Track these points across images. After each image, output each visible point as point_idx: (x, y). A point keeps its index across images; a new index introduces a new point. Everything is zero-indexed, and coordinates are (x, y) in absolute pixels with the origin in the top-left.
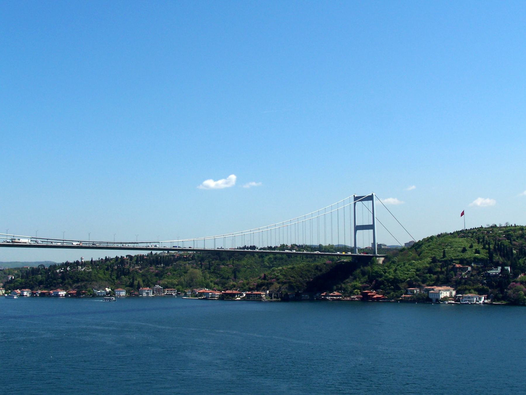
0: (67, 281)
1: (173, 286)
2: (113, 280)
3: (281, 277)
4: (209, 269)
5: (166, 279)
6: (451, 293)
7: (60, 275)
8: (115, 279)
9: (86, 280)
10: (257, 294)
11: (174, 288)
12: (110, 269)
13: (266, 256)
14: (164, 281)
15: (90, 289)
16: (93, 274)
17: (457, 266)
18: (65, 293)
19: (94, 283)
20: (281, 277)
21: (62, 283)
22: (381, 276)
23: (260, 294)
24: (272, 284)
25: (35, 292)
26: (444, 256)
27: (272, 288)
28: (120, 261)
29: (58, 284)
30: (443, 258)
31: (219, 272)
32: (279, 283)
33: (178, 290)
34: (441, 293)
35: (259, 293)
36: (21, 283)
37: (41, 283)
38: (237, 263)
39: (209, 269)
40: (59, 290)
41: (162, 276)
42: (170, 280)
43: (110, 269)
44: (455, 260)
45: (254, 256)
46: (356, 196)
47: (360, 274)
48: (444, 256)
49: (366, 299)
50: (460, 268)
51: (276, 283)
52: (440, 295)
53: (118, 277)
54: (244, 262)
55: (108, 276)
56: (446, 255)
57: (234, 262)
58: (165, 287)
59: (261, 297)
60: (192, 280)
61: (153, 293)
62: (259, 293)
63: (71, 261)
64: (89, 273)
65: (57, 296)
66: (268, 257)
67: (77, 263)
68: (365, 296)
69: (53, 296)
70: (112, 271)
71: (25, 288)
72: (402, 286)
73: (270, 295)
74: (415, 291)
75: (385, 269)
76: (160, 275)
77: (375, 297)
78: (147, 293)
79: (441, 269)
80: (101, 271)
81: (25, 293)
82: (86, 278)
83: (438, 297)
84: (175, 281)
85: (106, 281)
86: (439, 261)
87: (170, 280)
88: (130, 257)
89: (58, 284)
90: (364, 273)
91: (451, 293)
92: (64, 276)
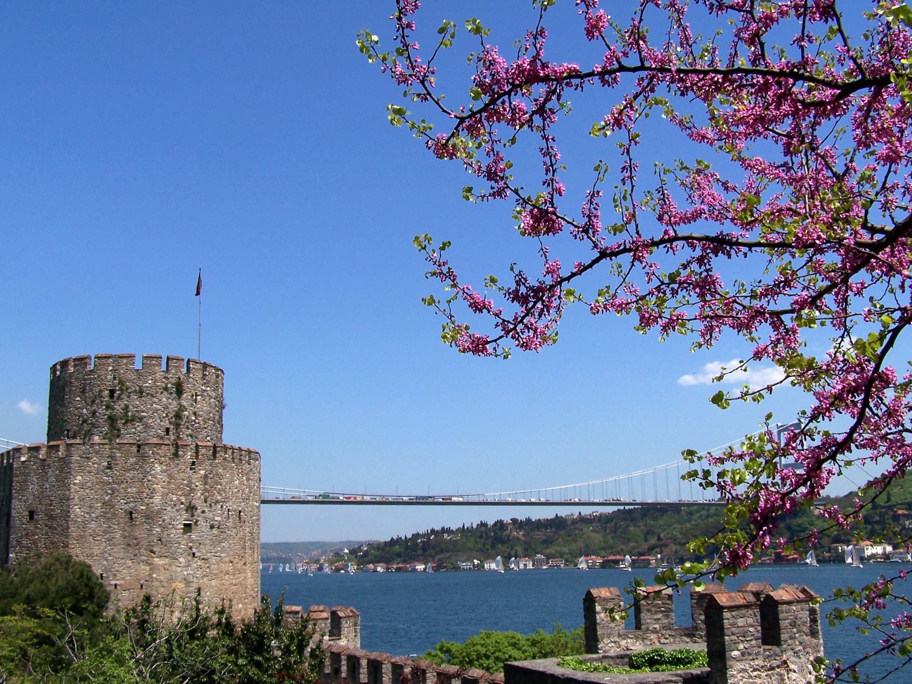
0: (428, 553)
1: (561, 555)
2: (487, 549)
3: (679, 536)
4: (615, 533)
5: (553, 547)
6: (884, 549)
7: (421, 545)
8: (490, 548)
9: (452, 551)
10: (644, 560)
11: (561, 557)
12: (485, 537)
13: (697, 512)
14: (551, 550)
15: (453, 561)
16: (460, 543)
17: (900, 512)
18: (424, 567)
19: (460, 553)
20: (679, 536)
21: (422, 555)
22: (804, 530)
23: (648, 560)
24: (666, 546)
25: (390, 566)
26: (889, 500)
27: (666, 551)
28: (500, 525)
29: (418, 555)
30: (887, 502)
31: (626, 536)
32: (675, 544)
33: (566, 561)
34: (867, 549)
35: (646, 557)
36: (376, 557)
37: (399, 555)
38: (652, 523)
39: (615, 533)
40: (416, 563)
41: (551, 543)
42: (559, 549)
43: (485, 537)
44: (902, 504)
45: (679, 511)
46: (779, 425)
47: (785, 531)
48: (889, 500)
49: (779, 559)
50: (904, 515)
51: (672, 545)
52: (866, 551)
53: (493, 547)
54: (661, 522)
55: (480, 546)
56: (893, 499)
57: (649, 522)
58: (549, 557)
59: (650, 564)
60: (587, 546)
61: (533, 565)
62: (646, 557)
63: (438, 528)
64: (456, 541)
65: (414, 570)
66: (698, 515)
67: (443, 531)
68: (778, 556)
69: (410, 571)
70: (487, 539)
71: (379, 562)
72: (825, 540)
73: (662, 560)
74: (840, 548)
75: (812, 521)
76: (548, 542)
77: (790, 557)
78: (525, 565)
79: (880, 517)
80: (472, 540)
81: (379, 569)
82: (451, 547)
83: (863, 555)
84: (565, 550)
85: (477, 551)
86: (883, 507)
87: (559, 549)
88: (514, 521)
89: (418, 555)
90: (789, 528)
91: (884, 549)
92: (426, 546)
